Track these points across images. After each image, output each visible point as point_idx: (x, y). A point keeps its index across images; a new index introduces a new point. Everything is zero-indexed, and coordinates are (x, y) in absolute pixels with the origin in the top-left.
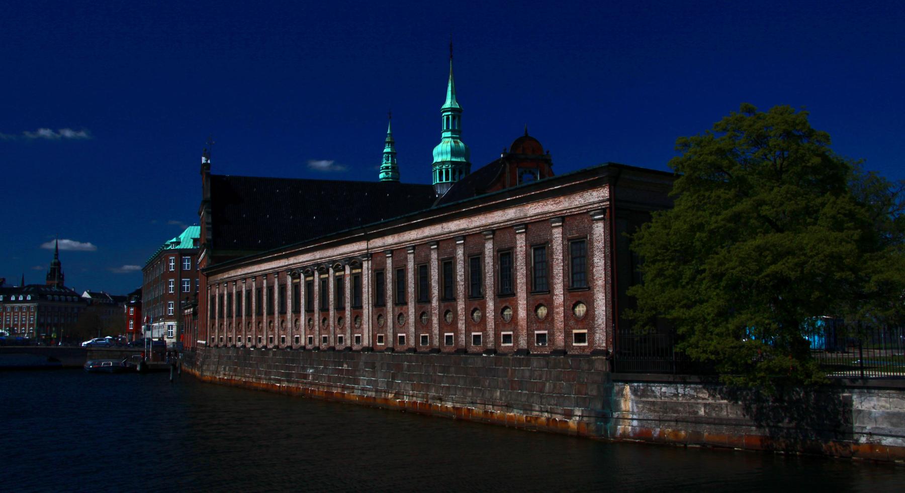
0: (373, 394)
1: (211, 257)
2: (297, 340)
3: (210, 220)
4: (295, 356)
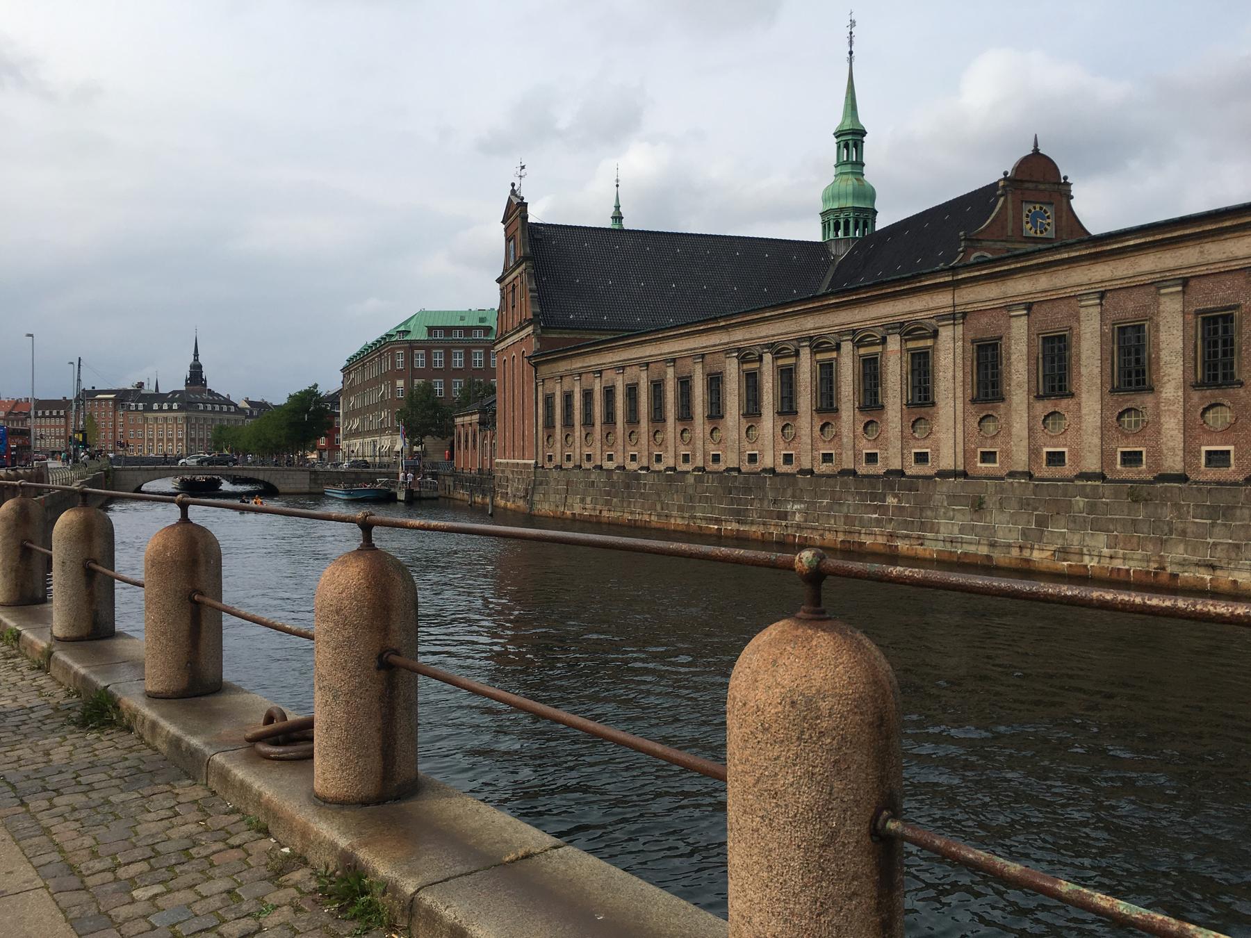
0: (984, 550)
1: (539, 339)
2: (753, 458)
3: (534, 286)
4: (743, 484)
